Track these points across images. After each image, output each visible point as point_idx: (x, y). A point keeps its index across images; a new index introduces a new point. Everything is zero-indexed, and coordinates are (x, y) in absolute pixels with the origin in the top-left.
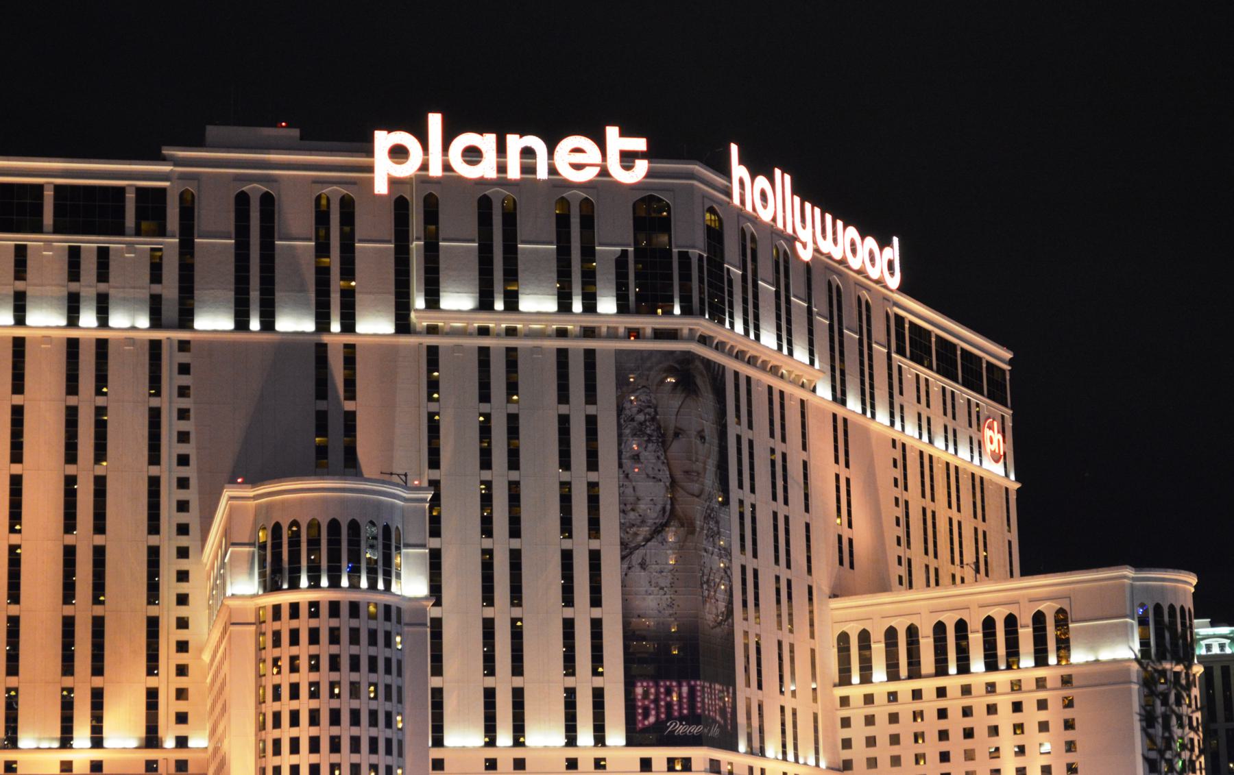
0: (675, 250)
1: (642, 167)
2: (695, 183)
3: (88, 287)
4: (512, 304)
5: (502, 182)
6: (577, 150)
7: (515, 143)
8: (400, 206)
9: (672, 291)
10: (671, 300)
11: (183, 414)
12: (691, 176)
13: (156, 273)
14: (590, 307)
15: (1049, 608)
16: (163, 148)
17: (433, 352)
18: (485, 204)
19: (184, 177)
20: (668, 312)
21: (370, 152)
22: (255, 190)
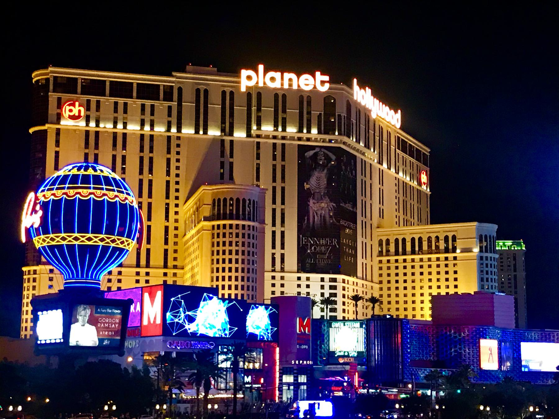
0: (337, 114)
1: (327, 86)
2: (344, 92)
3: (148, 117)
4: (284, 130)
5: (282, 89)
6: (307, 79)
7: (287, 76)
8: (249, 95)
10: (335, 131)
11: (178, 161)
12: (343, 89)
13: (170, 115)
14: (309, 132)
15: (450, 235)
16: (173, 72)
17: (258, 143)
18: (276, 96)
19: (179, 82)
20: (334, 134)
21: (239, 76)
22: (202, 88)
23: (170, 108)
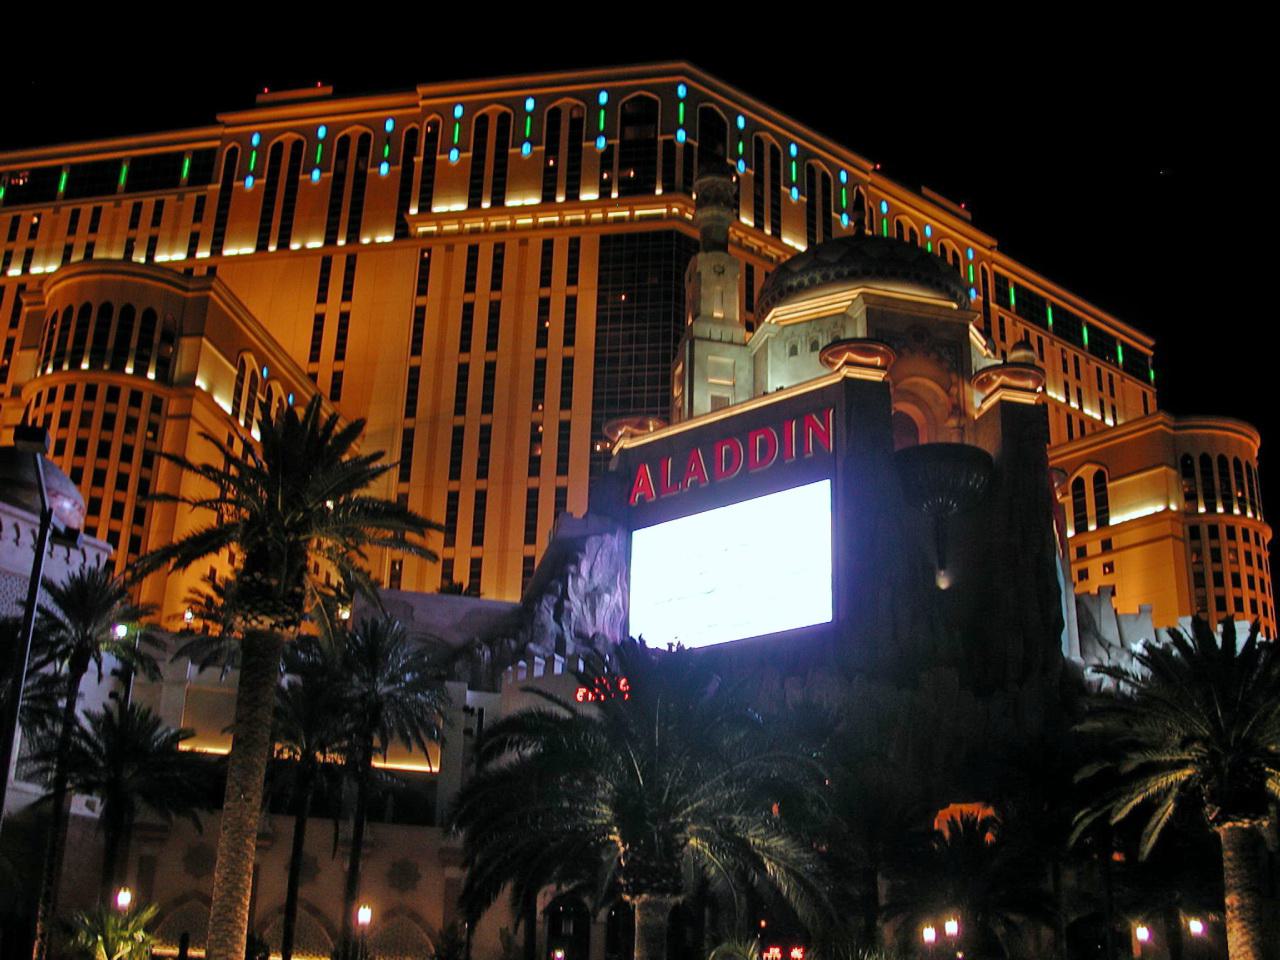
3: (143, 233)
4: (498, 202)
9: (655, 173)
14: (573, 196)
23: (201, 201)
